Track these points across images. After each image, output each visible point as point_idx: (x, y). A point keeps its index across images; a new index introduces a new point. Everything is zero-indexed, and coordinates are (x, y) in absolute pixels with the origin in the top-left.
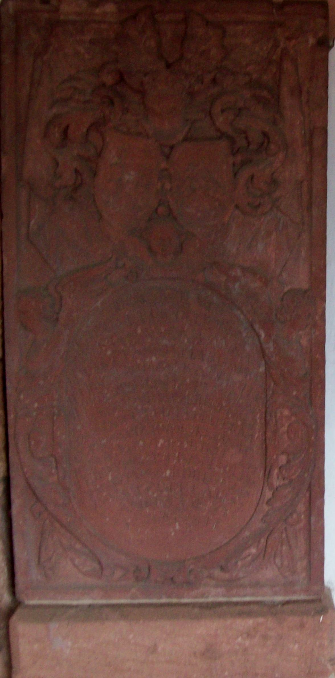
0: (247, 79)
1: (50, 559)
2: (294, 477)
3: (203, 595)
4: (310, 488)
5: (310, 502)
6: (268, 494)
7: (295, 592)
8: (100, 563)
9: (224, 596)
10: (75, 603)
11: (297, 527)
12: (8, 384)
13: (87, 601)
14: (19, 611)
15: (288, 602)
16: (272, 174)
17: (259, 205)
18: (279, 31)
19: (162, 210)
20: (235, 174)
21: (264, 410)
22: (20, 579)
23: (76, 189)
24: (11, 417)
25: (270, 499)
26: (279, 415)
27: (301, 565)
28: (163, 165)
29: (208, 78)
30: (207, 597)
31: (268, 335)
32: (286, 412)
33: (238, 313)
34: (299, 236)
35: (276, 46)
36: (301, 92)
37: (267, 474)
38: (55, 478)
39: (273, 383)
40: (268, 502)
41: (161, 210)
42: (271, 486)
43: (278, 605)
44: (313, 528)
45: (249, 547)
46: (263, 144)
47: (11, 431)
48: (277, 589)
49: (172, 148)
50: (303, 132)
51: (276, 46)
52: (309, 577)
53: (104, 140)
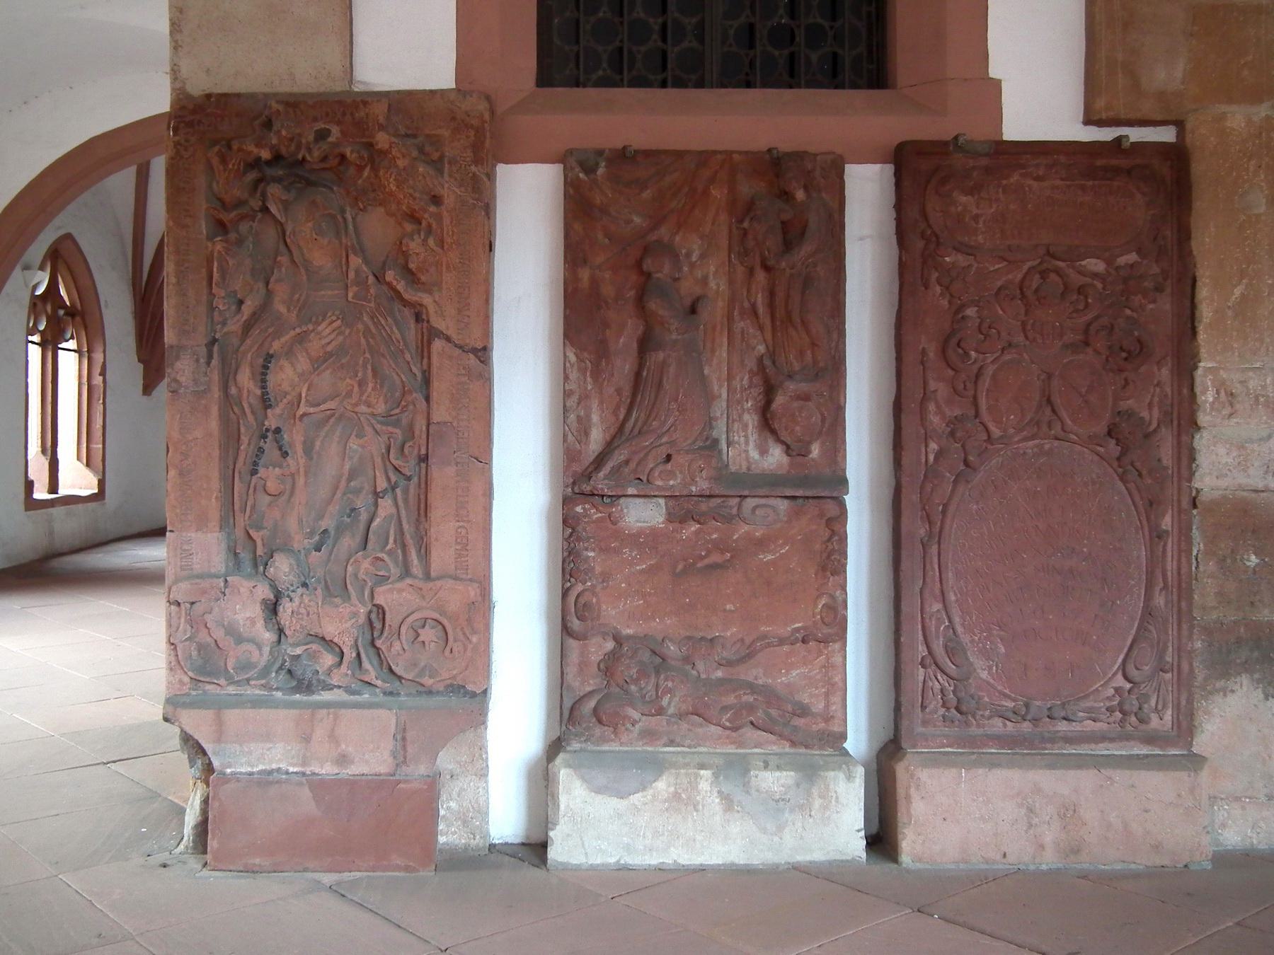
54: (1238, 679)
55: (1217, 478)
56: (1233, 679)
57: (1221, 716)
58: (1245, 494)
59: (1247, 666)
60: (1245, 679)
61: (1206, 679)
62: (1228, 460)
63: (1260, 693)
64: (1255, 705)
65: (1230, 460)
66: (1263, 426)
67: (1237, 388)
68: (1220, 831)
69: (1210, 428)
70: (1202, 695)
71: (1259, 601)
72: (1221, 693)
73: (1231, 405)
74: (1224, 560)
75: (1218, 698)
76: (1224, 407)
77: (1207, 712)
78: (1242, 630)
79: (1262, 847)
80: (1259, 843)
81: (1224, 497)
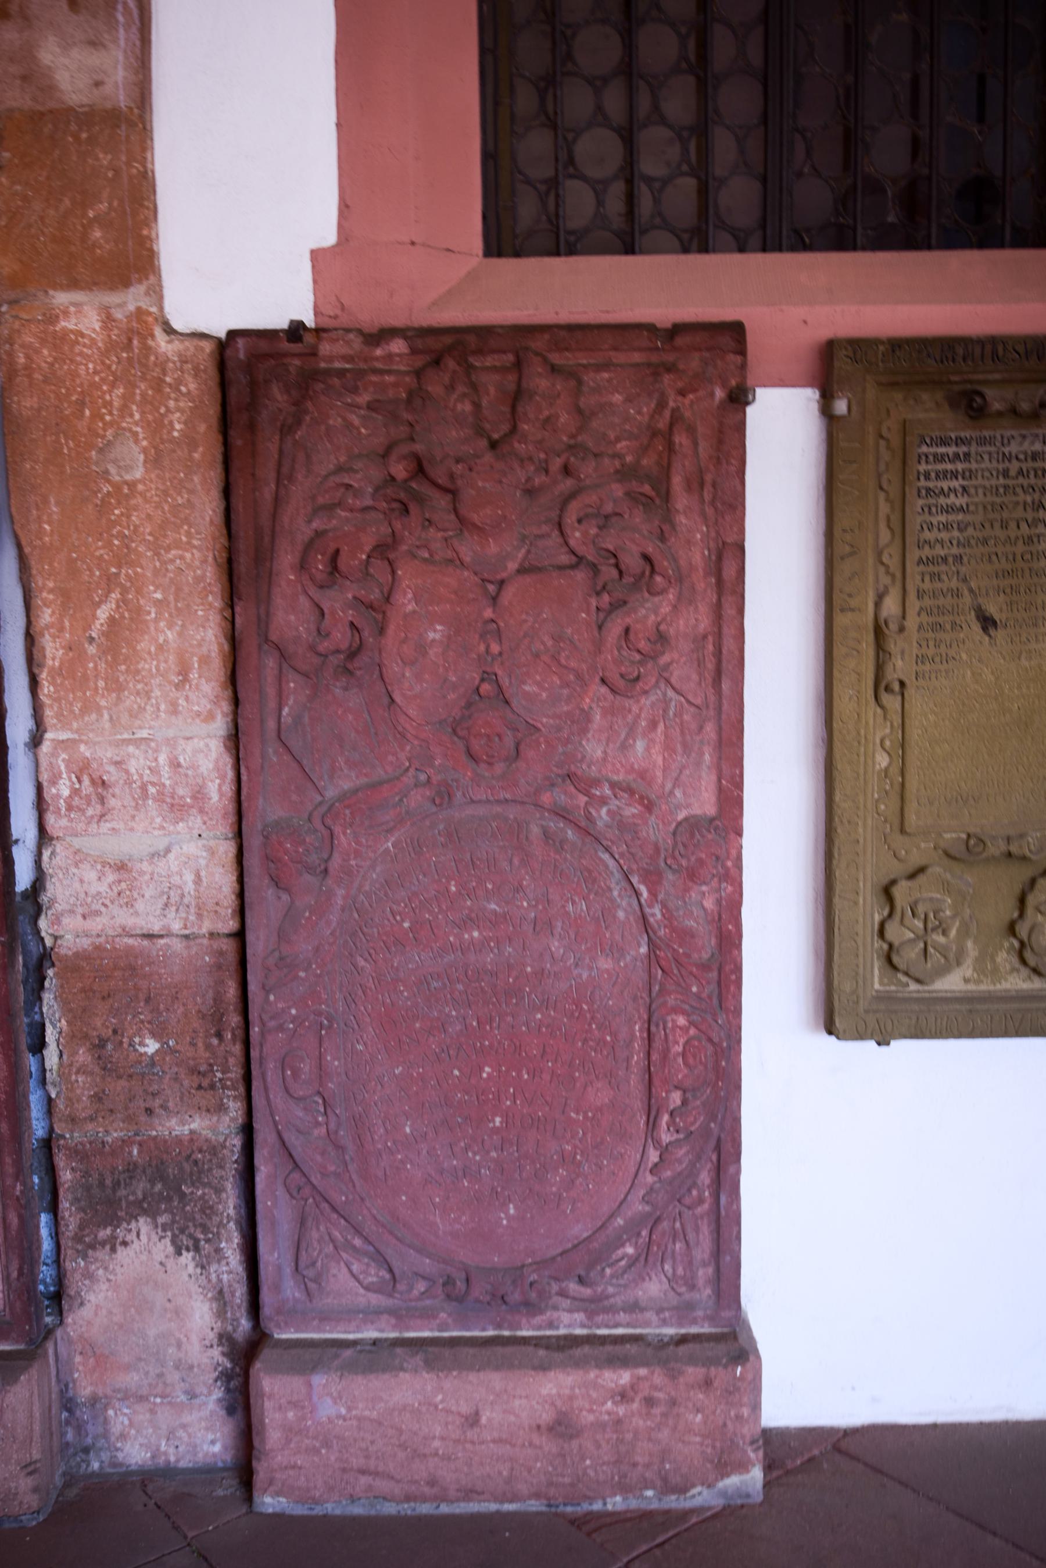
0: (617, 463)
1: (314, 1264)
2: (693, 1129)
3: (551, 1325)
4: (718, 1148)
5: (719, 1170)
6: (653, 1156)
7: (694, 1322)
8: (391, 1271)
9: (583, 1326)
10: (351, 1336)
11: (699, 1210)
12: (250, 977)
13: (371, 1334)
14: (267, 1355)
15: (683, 1340)
16: (659, 624)
17: (638, 678)
18: (667, 379)
19: (485, 688)
20: (600, 627)
21: (646, 1017)
22: (266, 1296)
23: (353, 654)
24: (255, 1030)
25: (656, 1165)
26: (670, 1025)
27: (703, 1274)
28: (488, 613)
29: (557, 463)
30: (557, 1328)
31: (653, 893)
32: (681, 1021)
33: (606, 857)
34: (701, 728)
35: (662, 405)
36: (702, 485)
37: (652, 1124)
38: (324, 1130)
39: (660, 972)
40: (655, 1170)
41: (485, 688)
42: (657, 1143)
43: (668, 1344)
44: (723, 1212)
45: (623, 1245)
46: (643, 573)
47: (254, 1054)
48: (667, 1314)
49: (502, 583)
50: (706, 553)
51: (662, 405)
52: (718, 1294)
53: (393, 572)
54: (133, 1225)
55: (84, 917)
56: (125, 1225)
57: (109, 1280)
58: (131, 941)
59: (145, 1205)
60: (143, 1224)
61: (81, 1227)
62: (101, 889)
63: (169, 1243)
64: (161, 1263)
65: (103, 888)
66: (156, 833)
67: (109, 772)
68: (119, 1445)
69: (68, 839)
70: (78, 1251)
71: (161, 1106)
72: (108, 1247)
73: (102, 800)
74: (102, 1044)
75: (102, 1254)
76: (89, 804)
77: (89, 1275)
78: (135, 1152)
79: (182, 1464)
80: (177, 1461)
81: (98, 948)
